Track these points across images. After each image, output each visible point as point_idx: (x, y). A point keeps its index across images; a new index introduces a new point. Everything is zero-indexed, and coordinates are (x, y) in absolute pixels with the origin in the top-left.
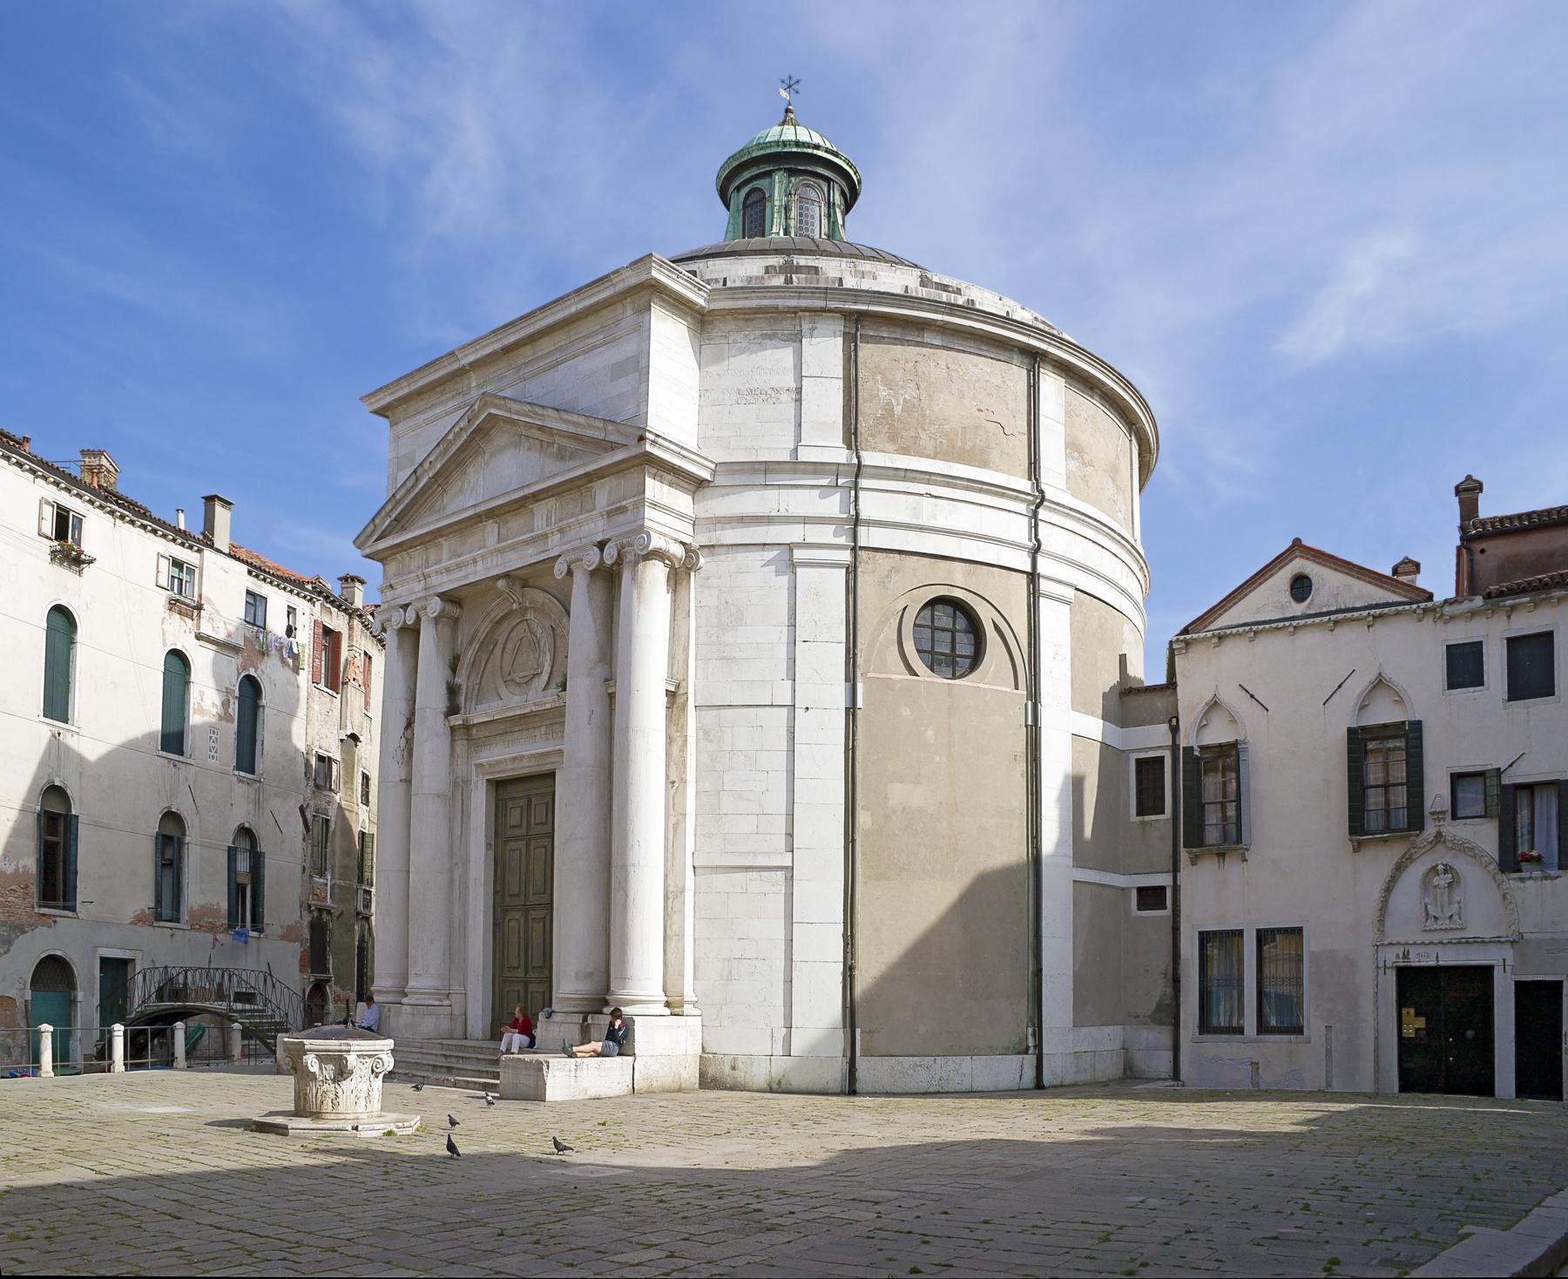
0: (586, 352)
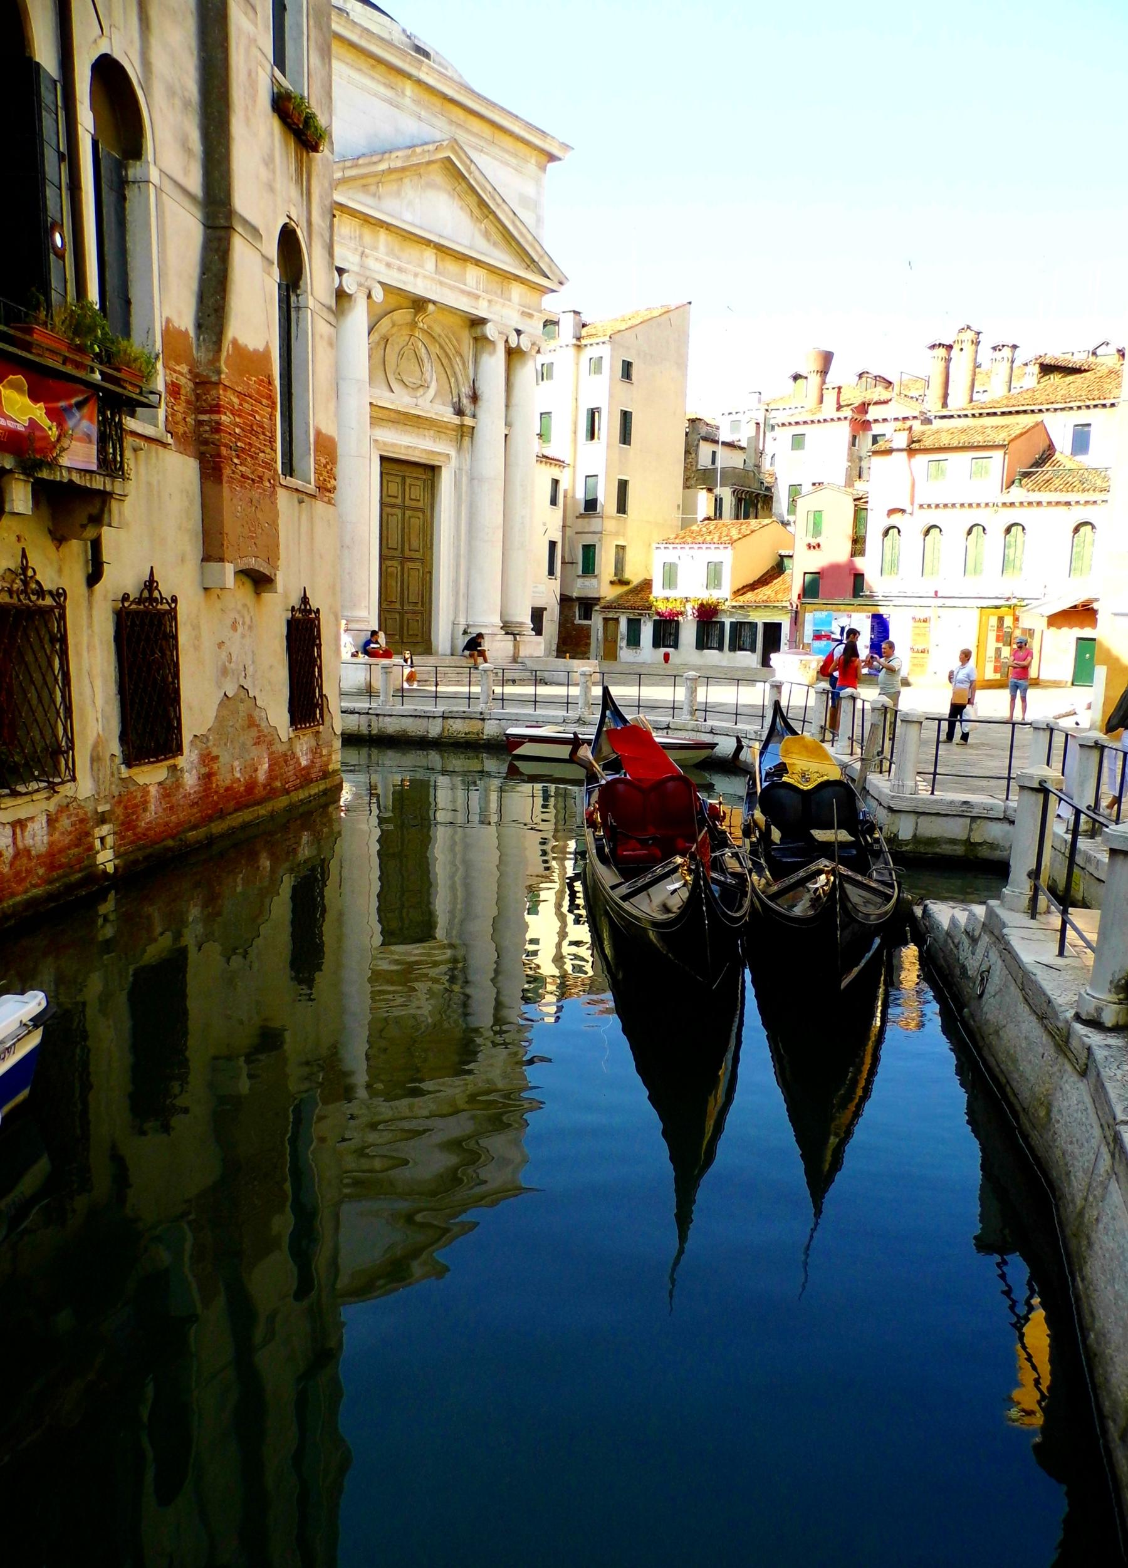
0: (502, 162)
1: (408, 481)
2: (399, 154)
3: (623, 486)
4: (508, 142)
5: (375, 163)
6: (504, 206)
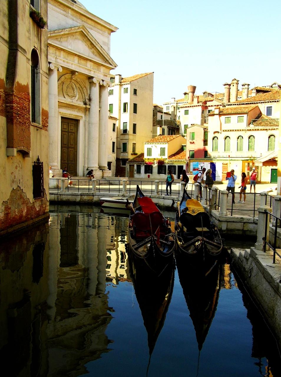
1: (70, 124)
2: (67, 30)
3: (135, 125)
4: (99, 27)
5: (60, 32)
6: (98, 44)
